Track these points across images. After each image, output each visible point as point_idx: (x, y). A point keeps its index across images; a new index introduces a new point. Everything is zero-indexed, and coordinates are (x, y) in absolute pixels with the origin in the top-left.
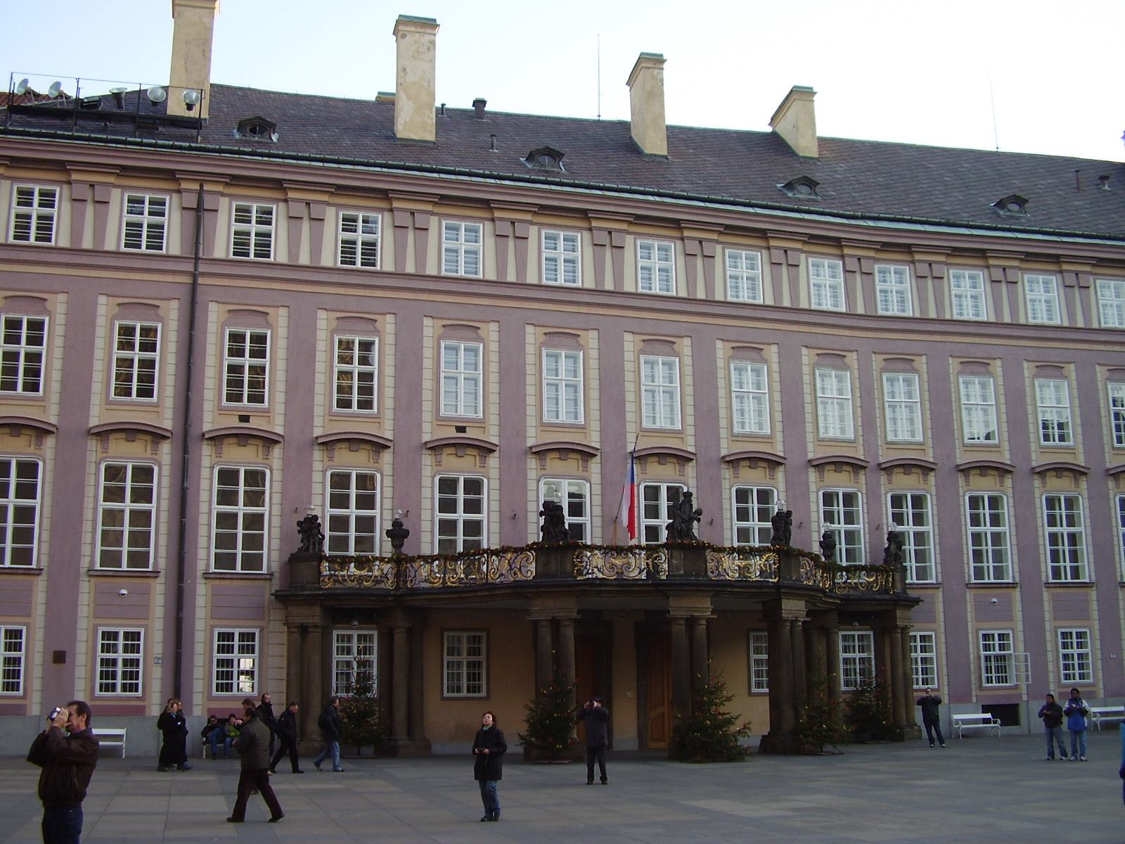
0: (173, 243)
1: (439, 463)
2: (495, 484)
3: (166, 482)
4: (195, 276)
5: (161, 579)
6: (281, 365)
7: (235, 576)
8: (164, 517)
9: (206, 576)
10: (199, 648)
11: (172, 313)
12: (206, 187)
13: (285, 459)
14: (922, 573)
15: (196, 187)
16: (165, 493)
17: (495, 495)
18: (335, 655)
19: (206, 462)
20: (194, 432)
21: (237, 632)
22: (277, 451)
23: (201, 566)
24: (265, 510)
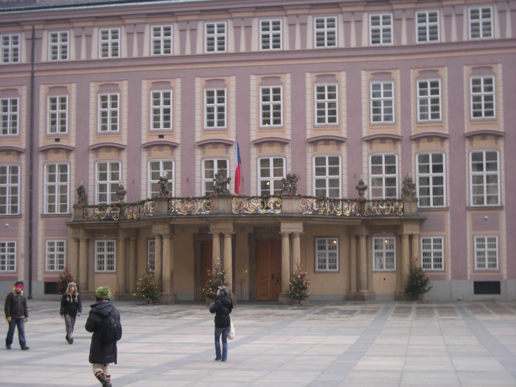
0: (23, 58)
1: (150, 155)
2: (179, 164)
3: (24, 173)
4: (33, 72)
5: (23, 218)
6: (74, 112)
7: (54, 216)
8: (24, 189)
9: (43, 216)
10: (40, 250)
11: (24, 91)
12: (36, 27)
13: (77, 159)
14: (439, 201)
15: (30, 27)
16: (24, 178)
17: (179, 169)
18: (96, 252)
19: (41, 162)
20: (35, 149)
21: (56, 242)
22: (72, 155)
23: (40, 212)
24: (68, 183)
